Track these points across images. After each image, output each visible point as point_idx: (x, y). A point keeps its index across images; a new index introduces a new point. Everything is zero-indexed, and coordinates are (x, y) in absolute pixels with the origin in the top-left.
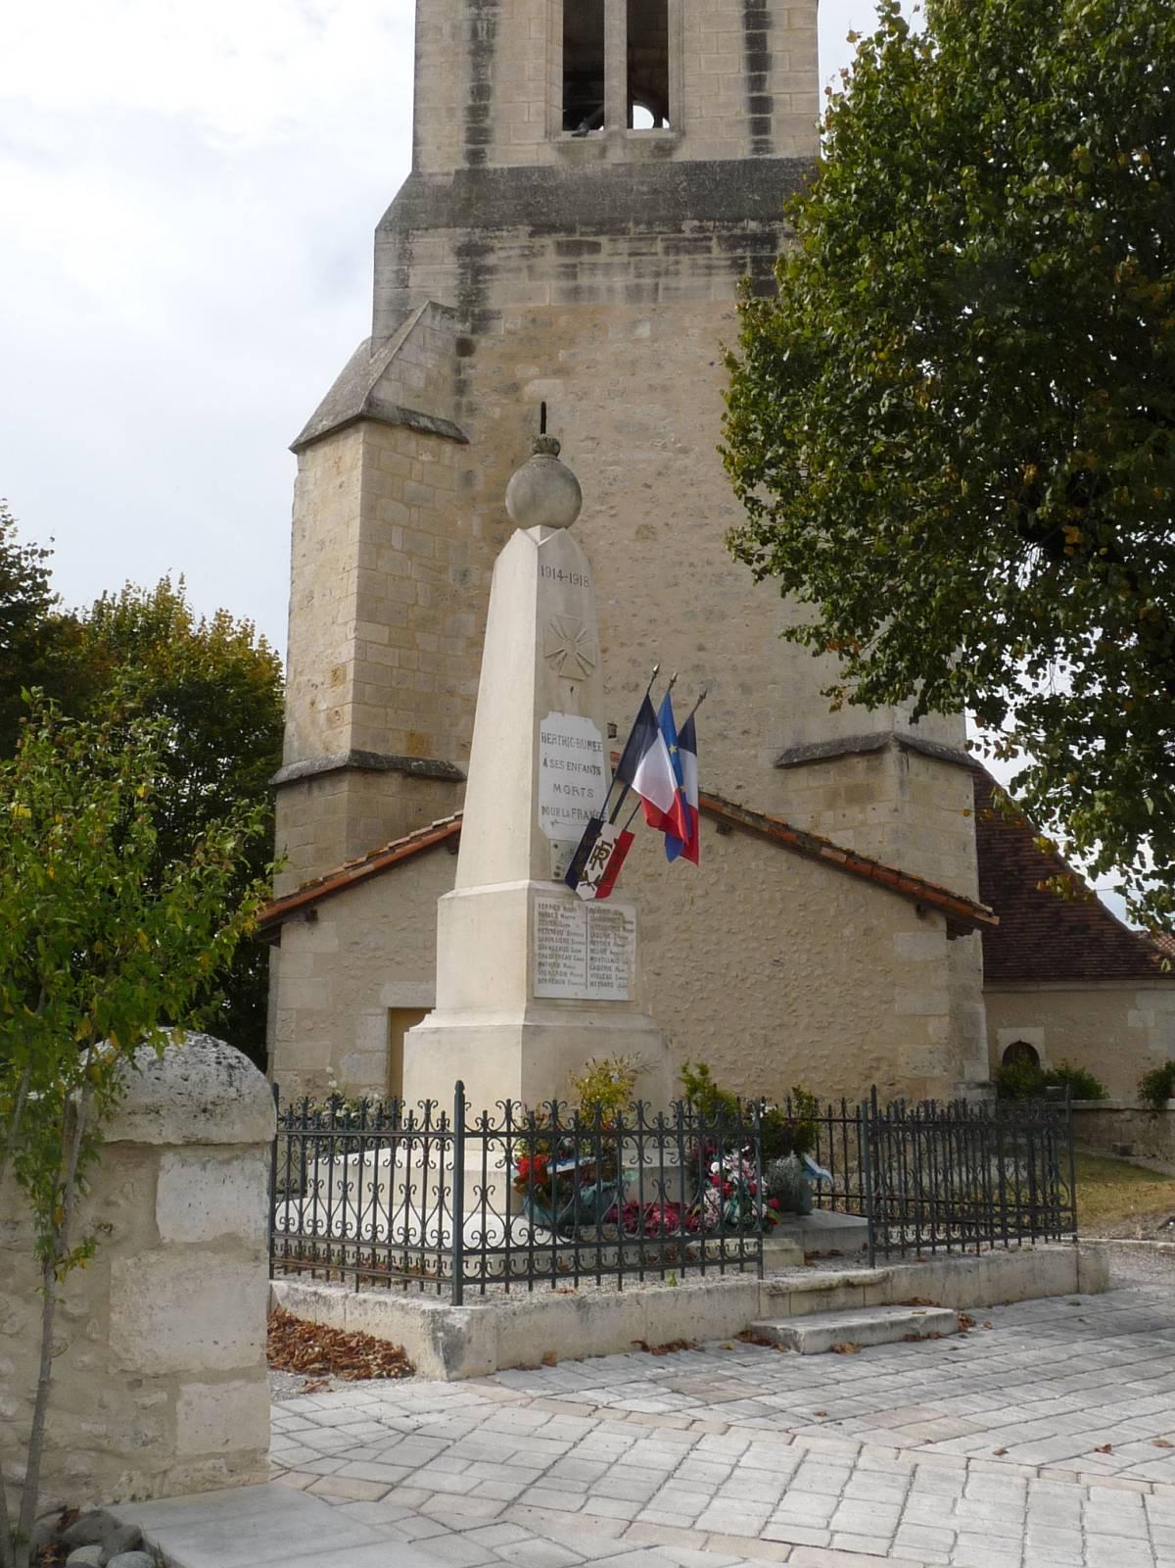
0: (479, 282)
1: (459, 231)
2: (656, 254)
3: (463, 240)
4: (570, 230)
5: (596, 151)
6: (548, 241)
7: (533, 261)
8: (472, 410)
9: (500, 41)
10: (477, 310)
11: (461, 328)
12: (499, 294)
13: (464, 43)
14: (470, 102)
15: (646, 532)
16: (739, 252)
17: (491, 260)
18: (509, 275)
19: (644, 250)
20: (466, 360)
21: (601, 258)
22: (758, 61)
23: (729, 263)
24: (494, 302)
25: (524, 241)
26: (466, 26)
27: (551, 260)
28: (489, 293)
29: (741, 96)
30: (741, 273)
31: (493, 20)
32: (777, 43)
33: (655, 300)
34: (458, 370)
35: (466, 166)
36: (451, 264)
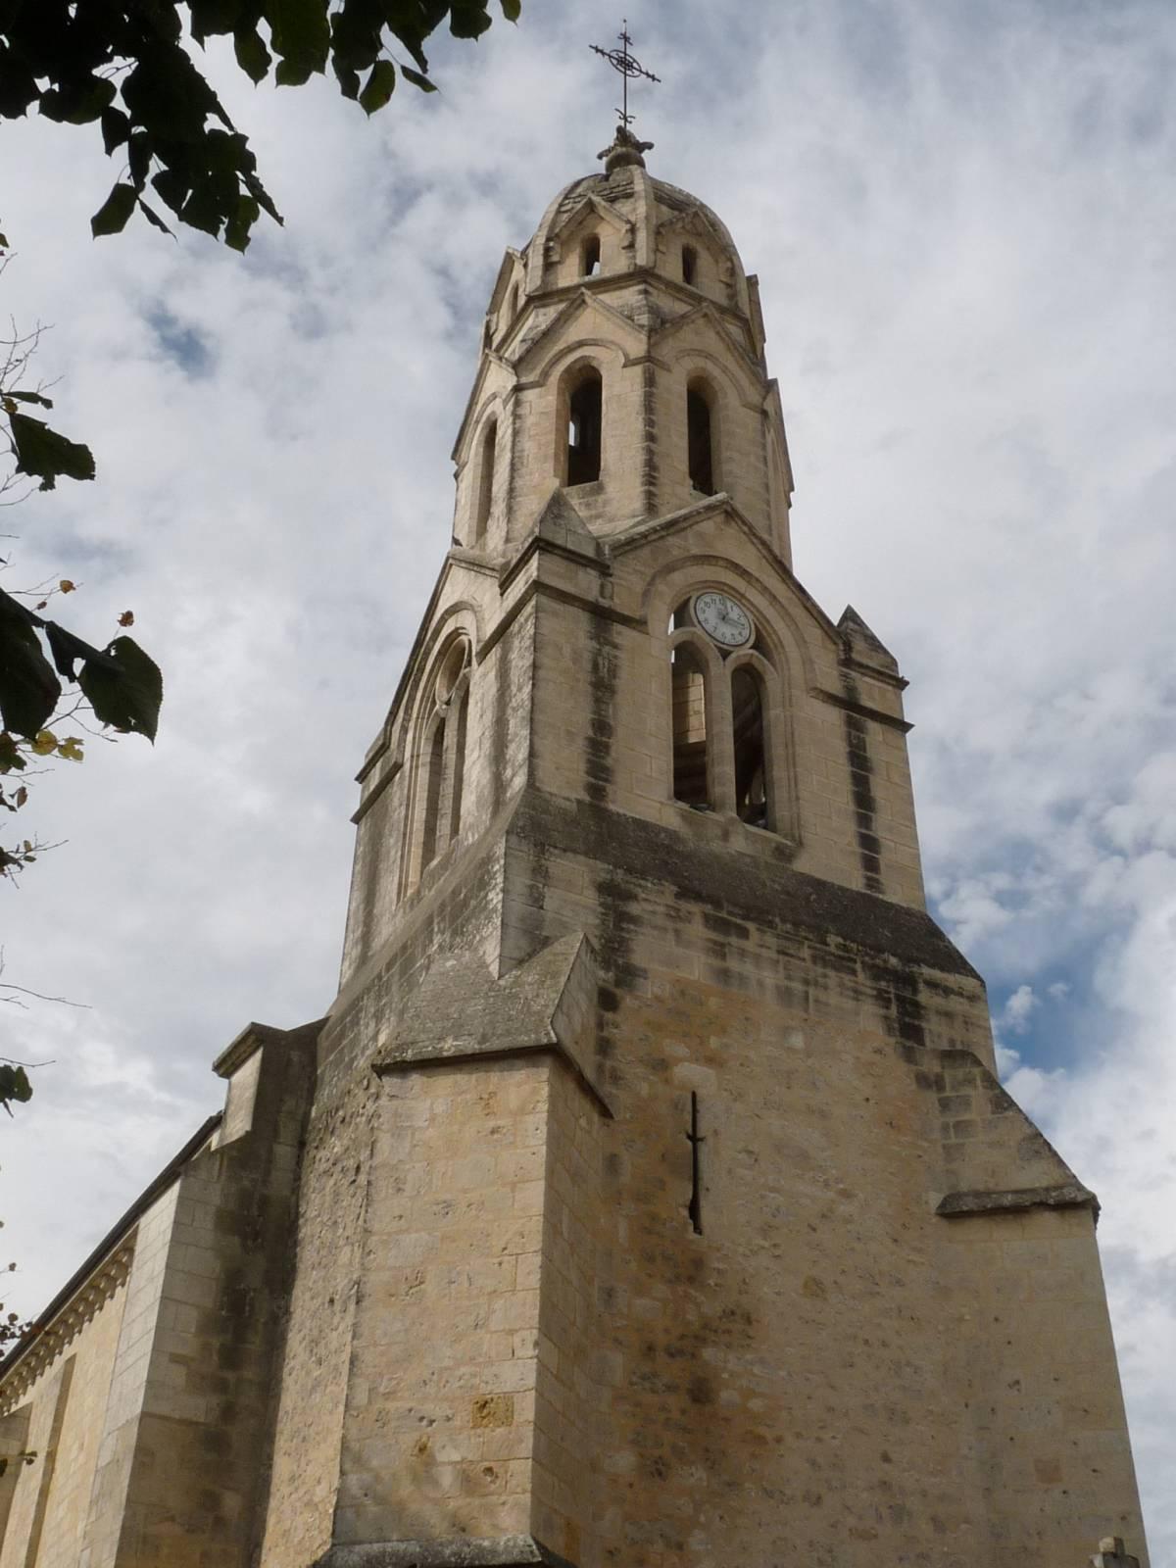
0: (622, 929)
1: (600, 865)
2: (804, 960)
3: (603, 876)
4: (717, 904)
5: (718, 832)
6: (696, 908)
7: (680, 925)
8: (616, 1078)
9: (622, 682)
10: (620, 961)
11: (606, 976)
12: (646, 949)
13: (585, 677)
14: (590, 733)
15: (814, 1288)
16: (883, 984)
17: (634, 908)
18: (655, 933)
19: (791, 952)
20: (609, 1016)
21: (750, 945)
22: (864, 801)
23: (875, 993)
24: (639, 957)
25: (670, 900)
26: (587, 656)
27: (697, 930)
28: (634, 945)
29: (851, 827)
30: (887, 1008)
31: (615, 661)
32: (879, 790)
33: (806, 1010)
34: (601, 1025)
35: (587, 799)
36: (590, 898)
